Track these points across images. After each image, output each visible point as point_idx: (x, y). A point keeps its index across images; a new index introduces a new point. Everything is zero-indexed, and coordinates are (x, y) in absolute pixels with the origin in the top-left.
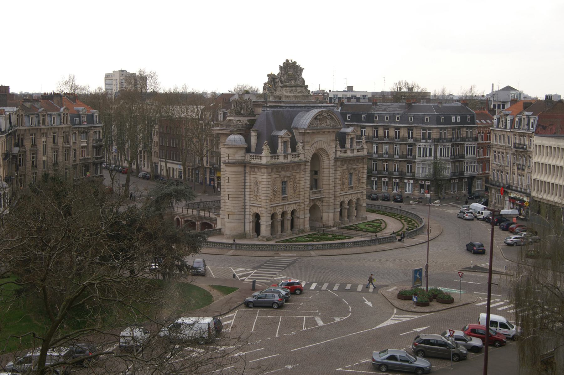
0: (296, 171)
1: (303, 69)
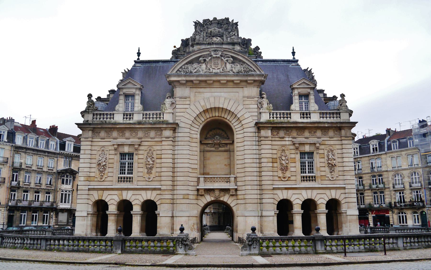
0: (151, 138)
1: (236, 24)
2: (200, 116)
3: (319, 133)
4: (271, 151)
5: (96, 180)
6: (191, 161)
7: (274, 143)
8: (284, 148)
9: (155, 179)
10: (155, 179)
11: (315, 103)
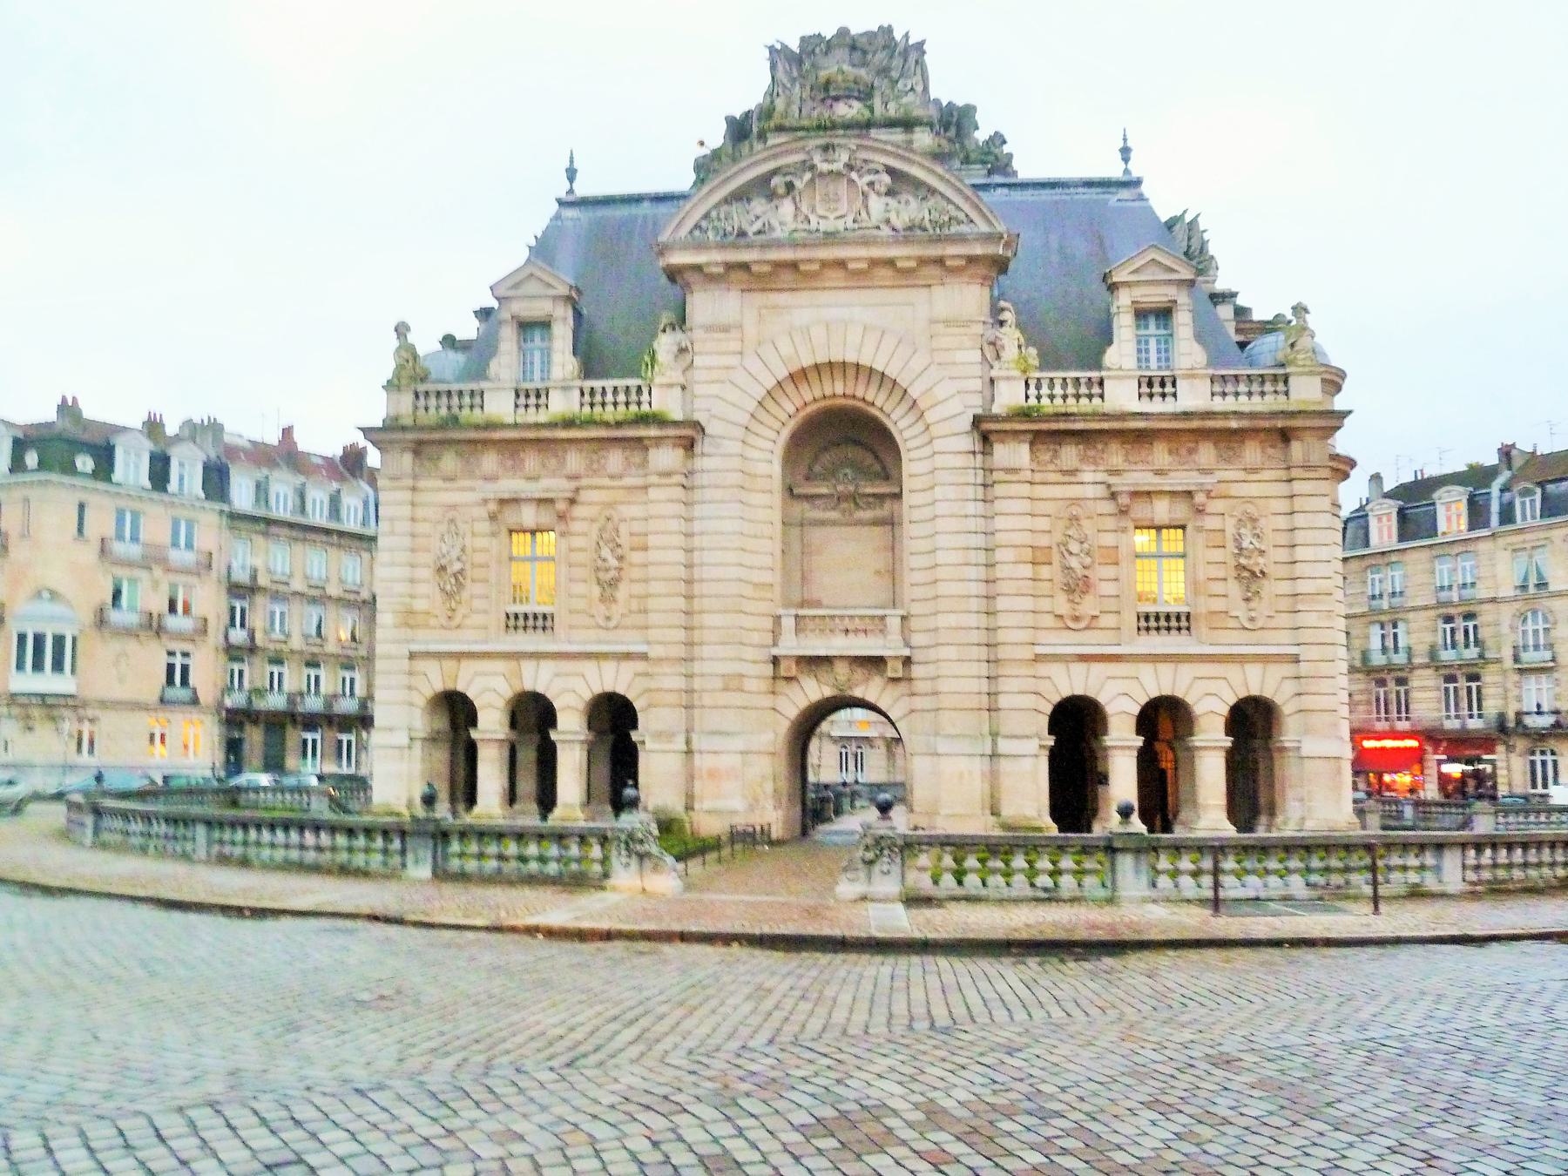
0: (612, 477)
2: (778, 394)
3: (1206, 453)
4: (1027, 522)
5: (433, 622)
6: (748, 559)
7: (1041, 491)
8: (1075, 511)
9: (628, 621)
10: (628, 621)
11: (1193, 339)
